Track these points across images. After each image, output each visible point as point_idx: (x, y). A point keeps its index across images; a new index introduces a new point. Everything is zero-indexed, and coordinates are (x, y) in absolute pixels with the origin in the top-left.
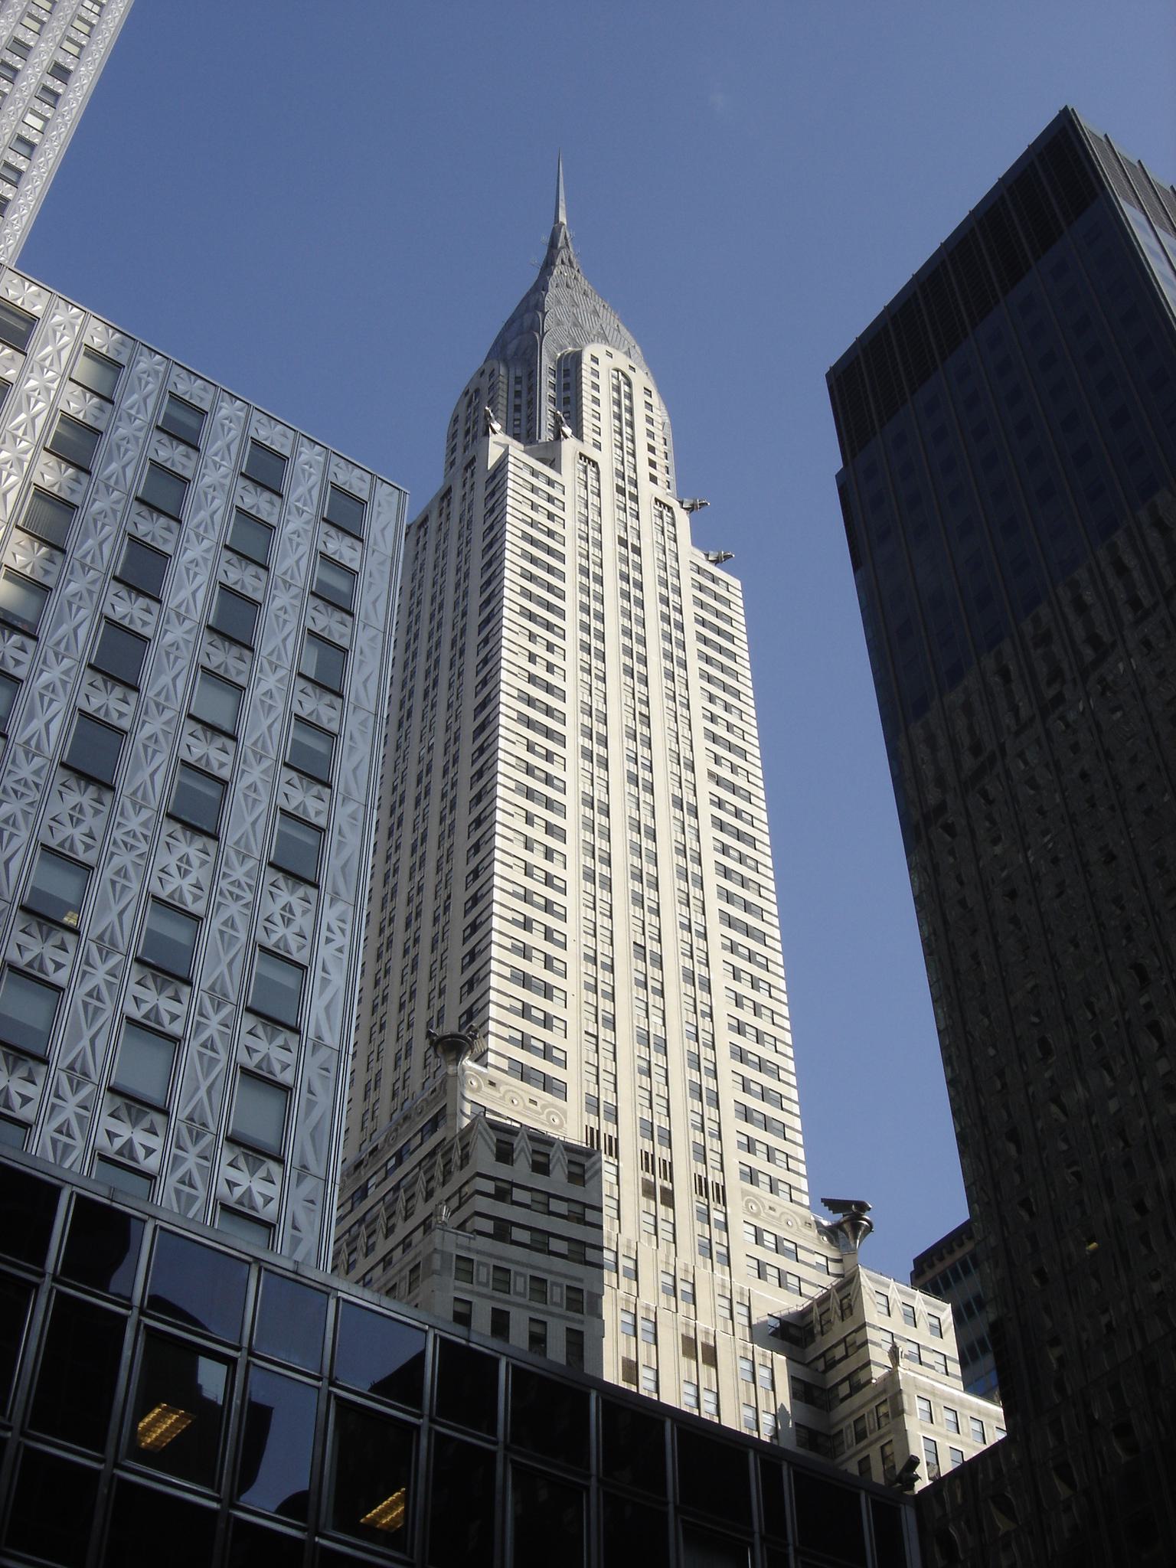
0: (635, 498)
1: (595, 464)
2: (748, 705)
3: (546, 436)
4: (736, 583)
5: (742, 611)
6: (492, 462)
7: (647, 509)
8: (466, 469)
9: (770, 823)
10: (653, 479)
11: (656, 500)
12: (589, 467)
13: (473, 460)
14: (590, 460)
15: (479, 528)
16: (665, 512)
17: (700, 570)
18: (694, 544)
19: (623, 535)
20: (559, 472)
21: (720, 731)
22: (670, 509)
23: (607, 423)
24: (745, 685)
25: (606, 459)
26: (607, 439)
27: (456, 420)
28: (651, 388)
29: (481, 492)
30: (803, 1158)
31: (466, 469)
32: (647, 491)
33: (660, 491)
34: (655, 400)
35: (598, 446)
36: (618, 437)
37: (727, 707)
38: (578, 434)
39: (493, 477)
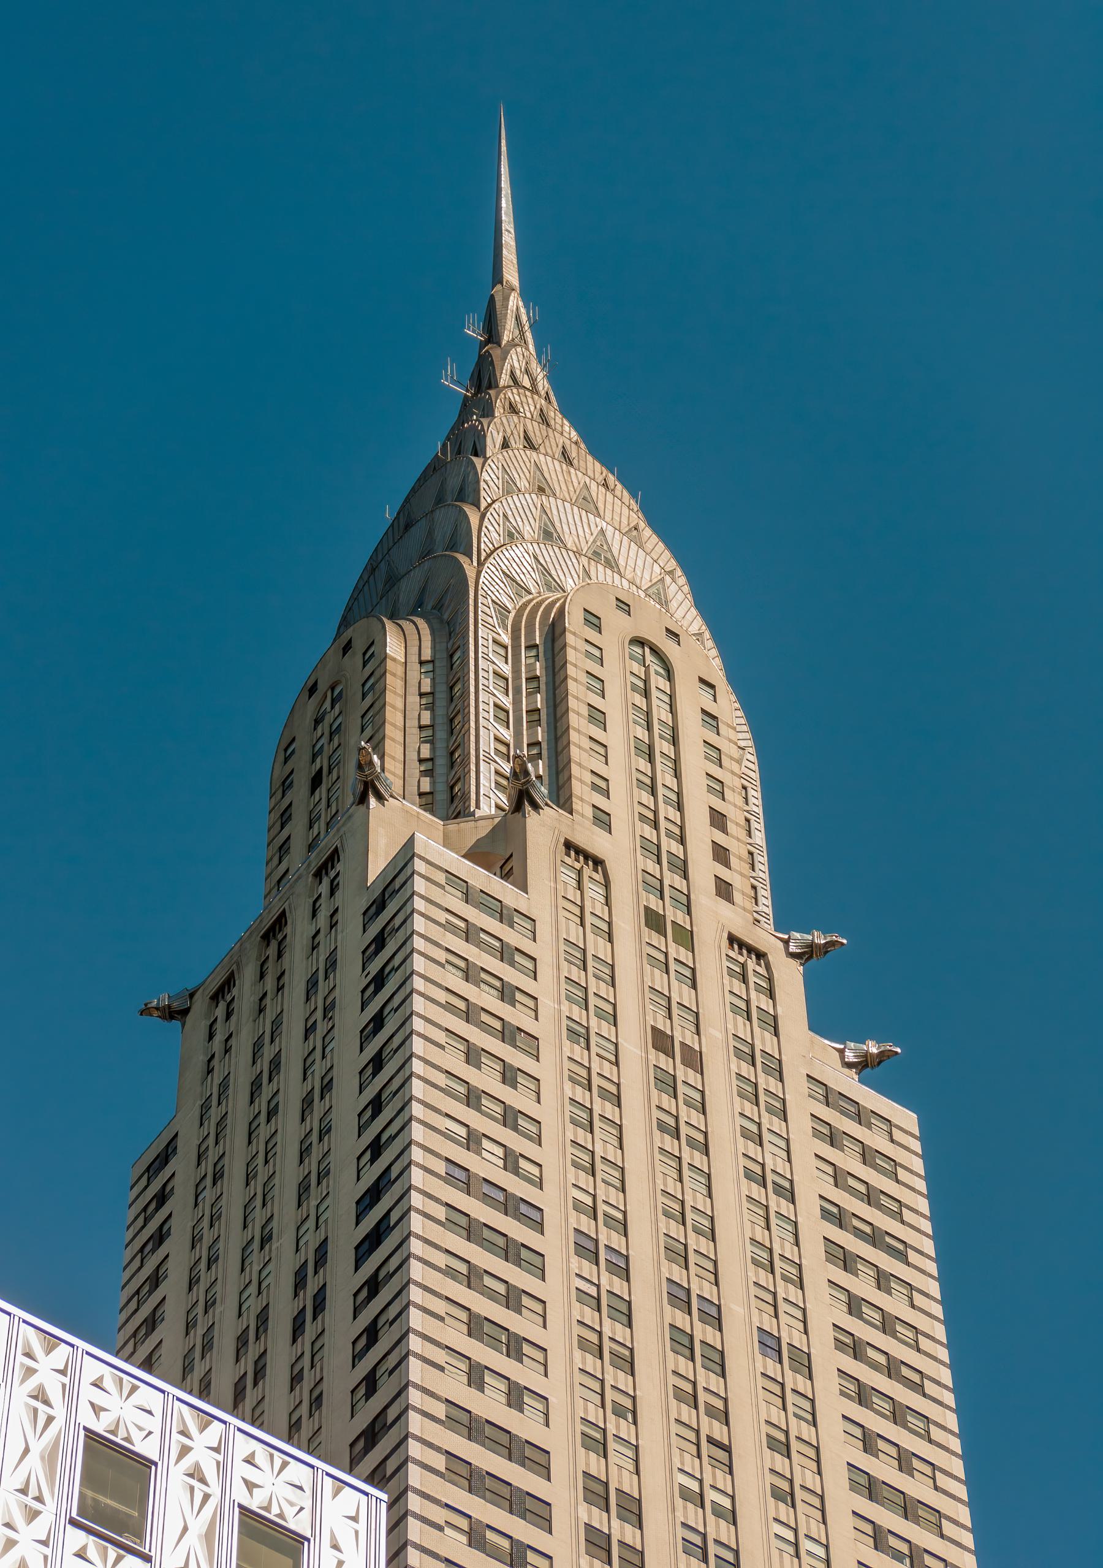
0: (686, 938)
1: (598, 863)
2: (924, 1273)
3: (489, 799)
4: (907, 1119)
5: (921, 1185)
6: (377, 865)
7: (712, 960)
8: (318, 875)
9: (929, 1177)
10: (724, 890)
11: (732, 939)
12: (588, 871)
13: (334, 856)
14: (587, 856)
15: (348, 1101)
16: (751, 964)
17: (829, 1097)
18: (812, 1028)
19: (662, 1024)
20: (523, 886)
21: (884, 1470)
22: (760, 956)
23: (621, 769)
24: (918, 1232)
25: (618, 848)
26: (622, 804)
27: (287, 751)
28: (718, 676)
29: (352, 938)
30: (965, 1498)
31: (318, 875)
32: (714, 919)
33: (734, 918)
34: (728, 706)
35: (603, 819)
36: (646, 798)
37: (883, 1280)
38: (562, 798)
39: (380, 904)
